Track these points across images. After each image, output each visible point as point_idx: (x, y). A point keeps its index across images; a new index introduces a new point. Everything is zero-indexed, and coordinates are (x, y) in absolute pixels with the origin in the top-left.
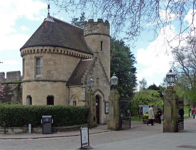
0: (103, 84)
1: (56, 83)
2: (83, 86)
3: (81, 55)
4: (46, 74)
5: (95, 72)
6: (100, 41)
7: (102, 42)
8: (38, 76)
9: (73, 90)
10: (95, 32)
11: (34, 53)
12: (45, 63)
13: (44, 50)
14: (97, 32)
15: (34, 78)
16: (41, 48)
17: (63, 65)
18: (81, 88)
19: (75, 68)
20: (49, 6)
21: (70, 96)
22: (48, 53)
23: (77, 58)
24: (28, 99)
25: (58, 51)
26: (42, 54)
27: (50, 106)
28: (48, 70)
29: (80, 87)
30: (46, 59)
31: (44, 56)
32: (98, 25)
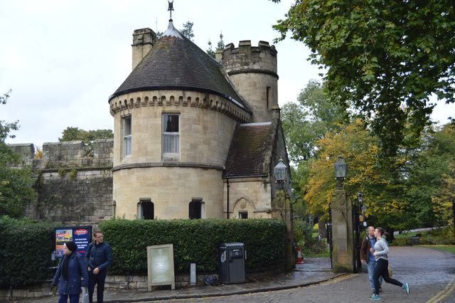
1: (209, 171)
2: (268, 180)
4: (188, 150)
6: (265, 86)
8: (168, 155)
10: (256, 67)
11: (160, 104)
13: (185, 100)
15: (159, 160)
16: (180, 93)
18: (260, 183)
20: (171, 7)
21: (231, 202)
22: (193, 105)
24: (140, 207)
25: (212, 101)
26: (180, 109)
27: (195, 221)
28: (192, 142)
30: (189, 119)
31: (183, 112)
32: (262, 55)
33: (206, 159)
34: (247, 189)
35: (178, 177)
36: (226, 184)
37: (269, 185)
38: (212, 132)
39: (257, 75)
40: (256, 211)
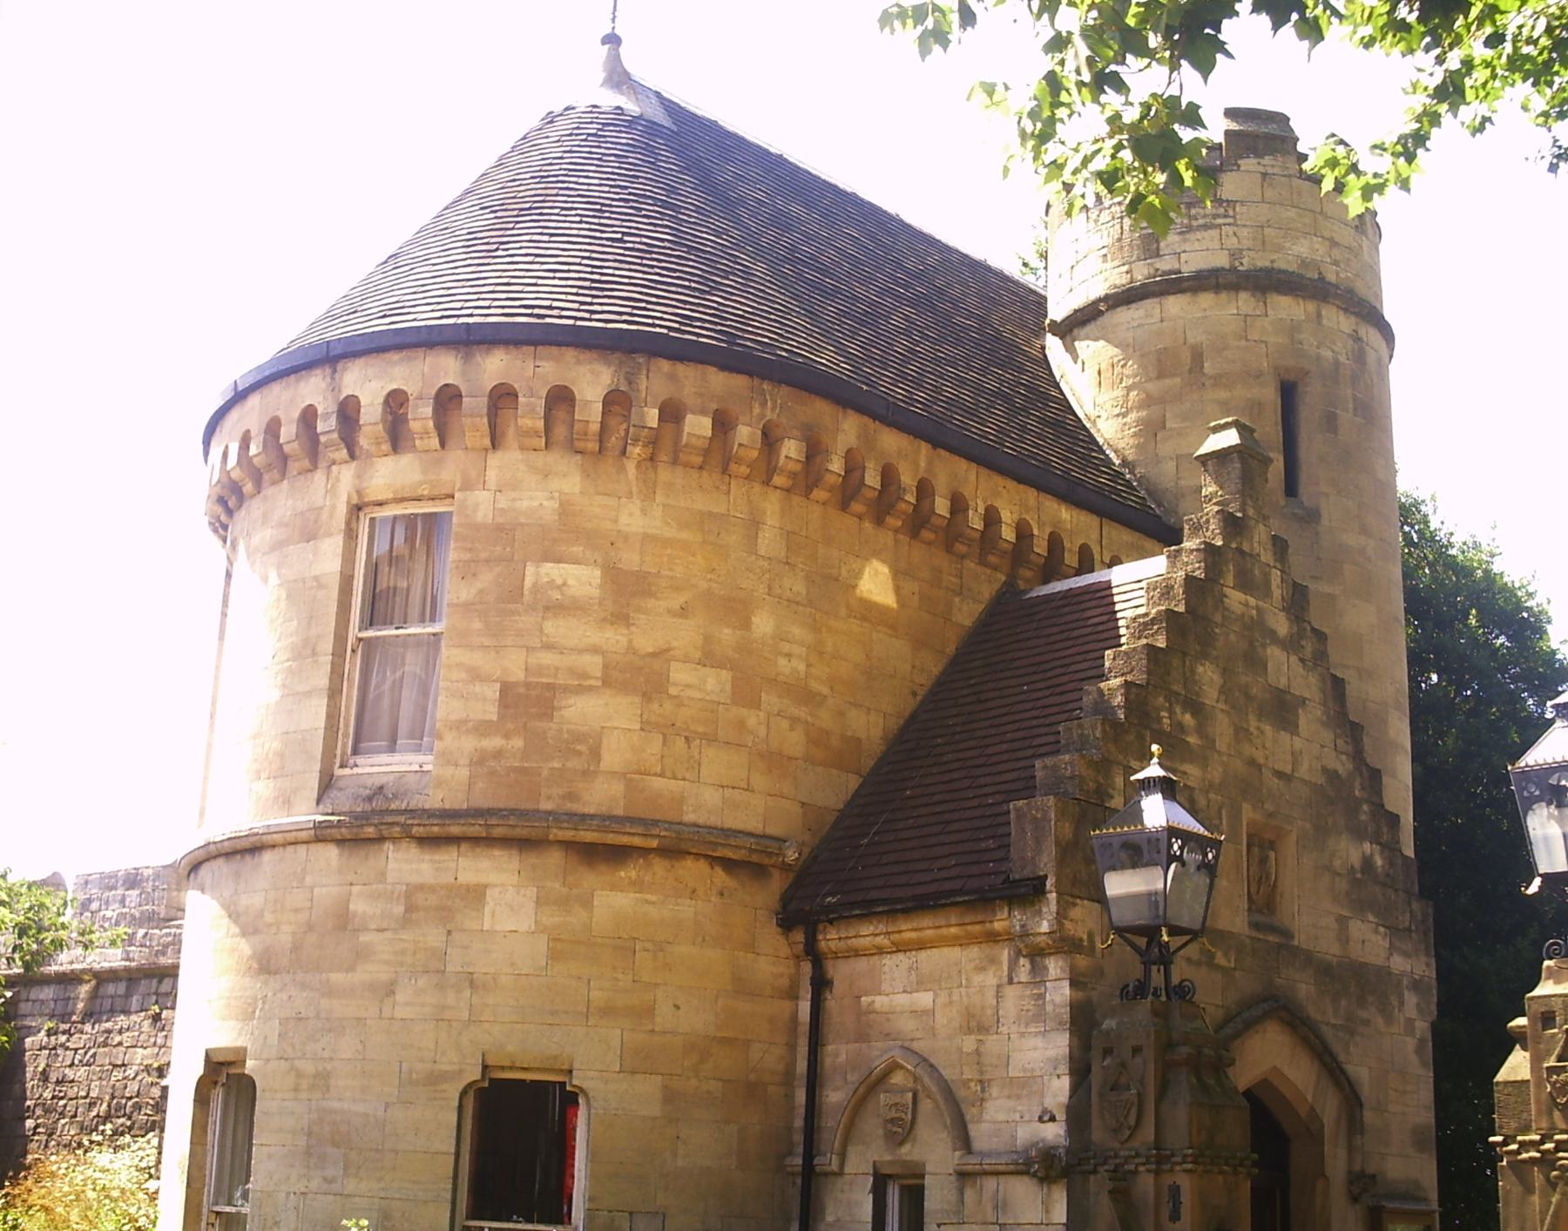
0: (1342, 921)
3: (1007, 516)
4: (482, 728)
5: (1222, 728)
7: (1288, 392)
9: (880, 1002)
12: (487, 578)
14: (1221, 260)
17: (746, 625)
19: (924, 681)
21: (834, 1097)
23: (949, 549)
28: (518, 675)
29: (992, 938)
33: (618, 788)
34: (925, 999)
35: (399, 909)
36: (807, 968)
37: (1055, 967)
38: (683, 612)
39: (1206, 299)
40: (972, 1163)
